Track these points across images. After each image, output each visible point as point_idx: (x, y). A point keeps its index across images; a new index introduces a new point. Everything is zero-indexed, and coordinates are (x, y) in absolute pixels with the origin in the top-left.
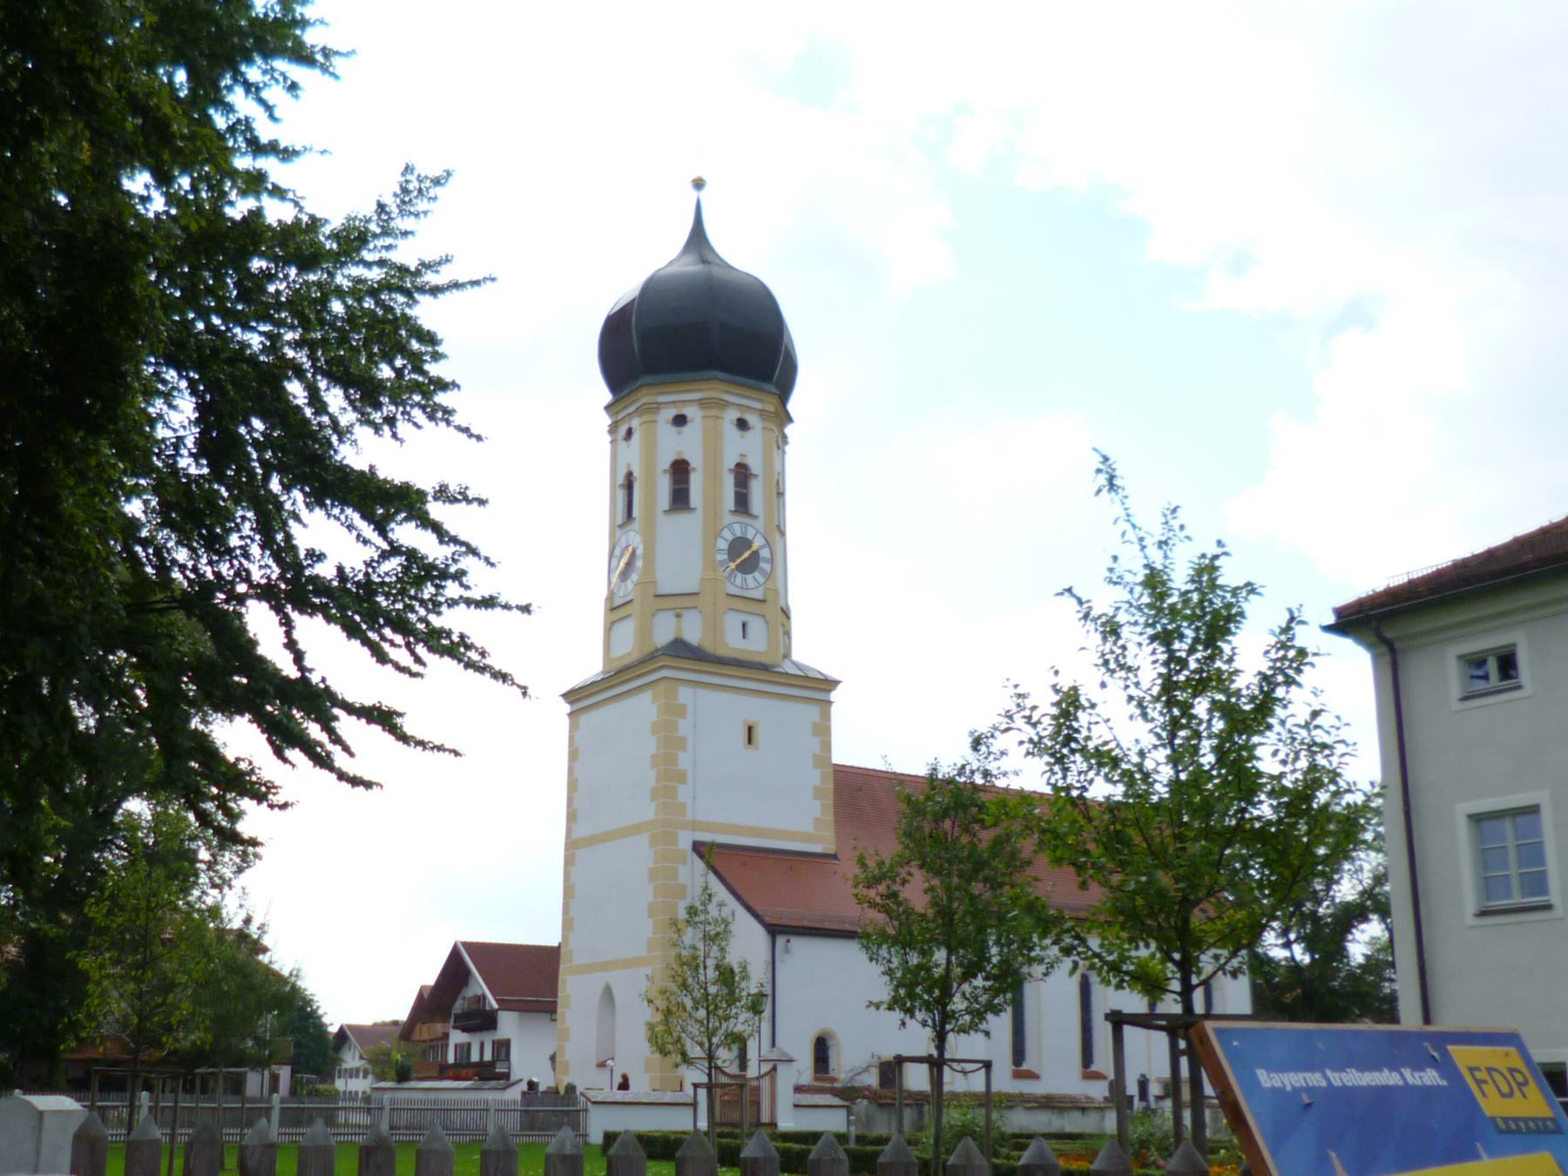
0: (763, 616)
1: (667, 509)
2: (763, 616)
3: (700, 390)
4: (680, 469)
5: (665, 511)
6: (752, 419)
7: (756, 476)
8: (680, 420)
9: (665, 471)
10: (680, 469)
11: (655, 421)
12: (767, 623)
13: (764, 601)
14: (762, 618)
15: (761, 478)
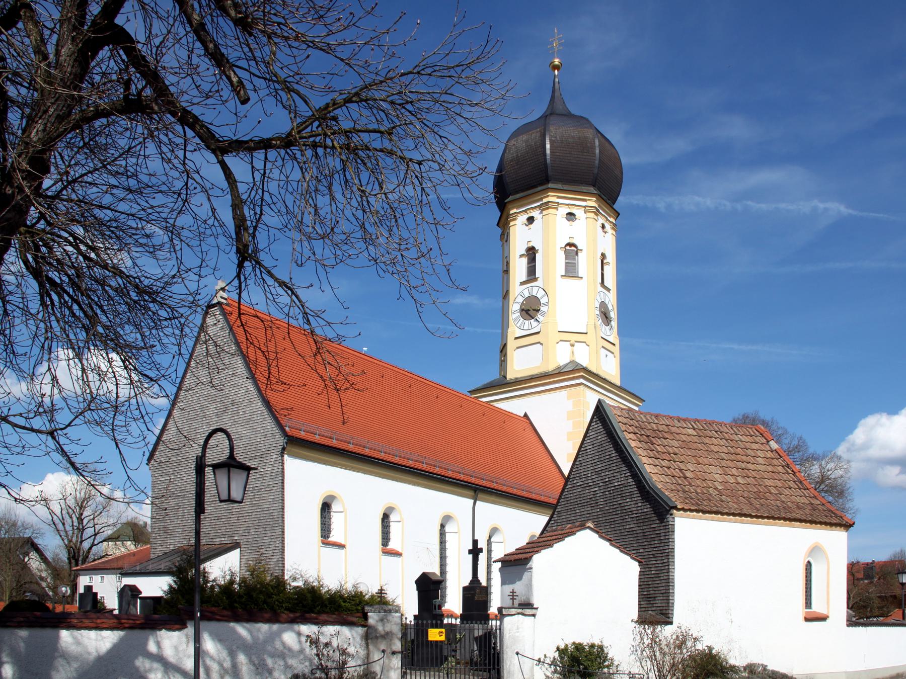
0: (585, 342)
1: (524, 278)
2: (585, 342)
3: (541, 199)
4: (531, 253)
5: (522, 283)
6: (579, 212)
7: (581, 250)
8: (531, 220)
9: (521, 256)
10: (531, 253)
11: (515, 225)
12: (588, 346)
13: (586, 333)
14: (585, 344)
15: (584, 251)
